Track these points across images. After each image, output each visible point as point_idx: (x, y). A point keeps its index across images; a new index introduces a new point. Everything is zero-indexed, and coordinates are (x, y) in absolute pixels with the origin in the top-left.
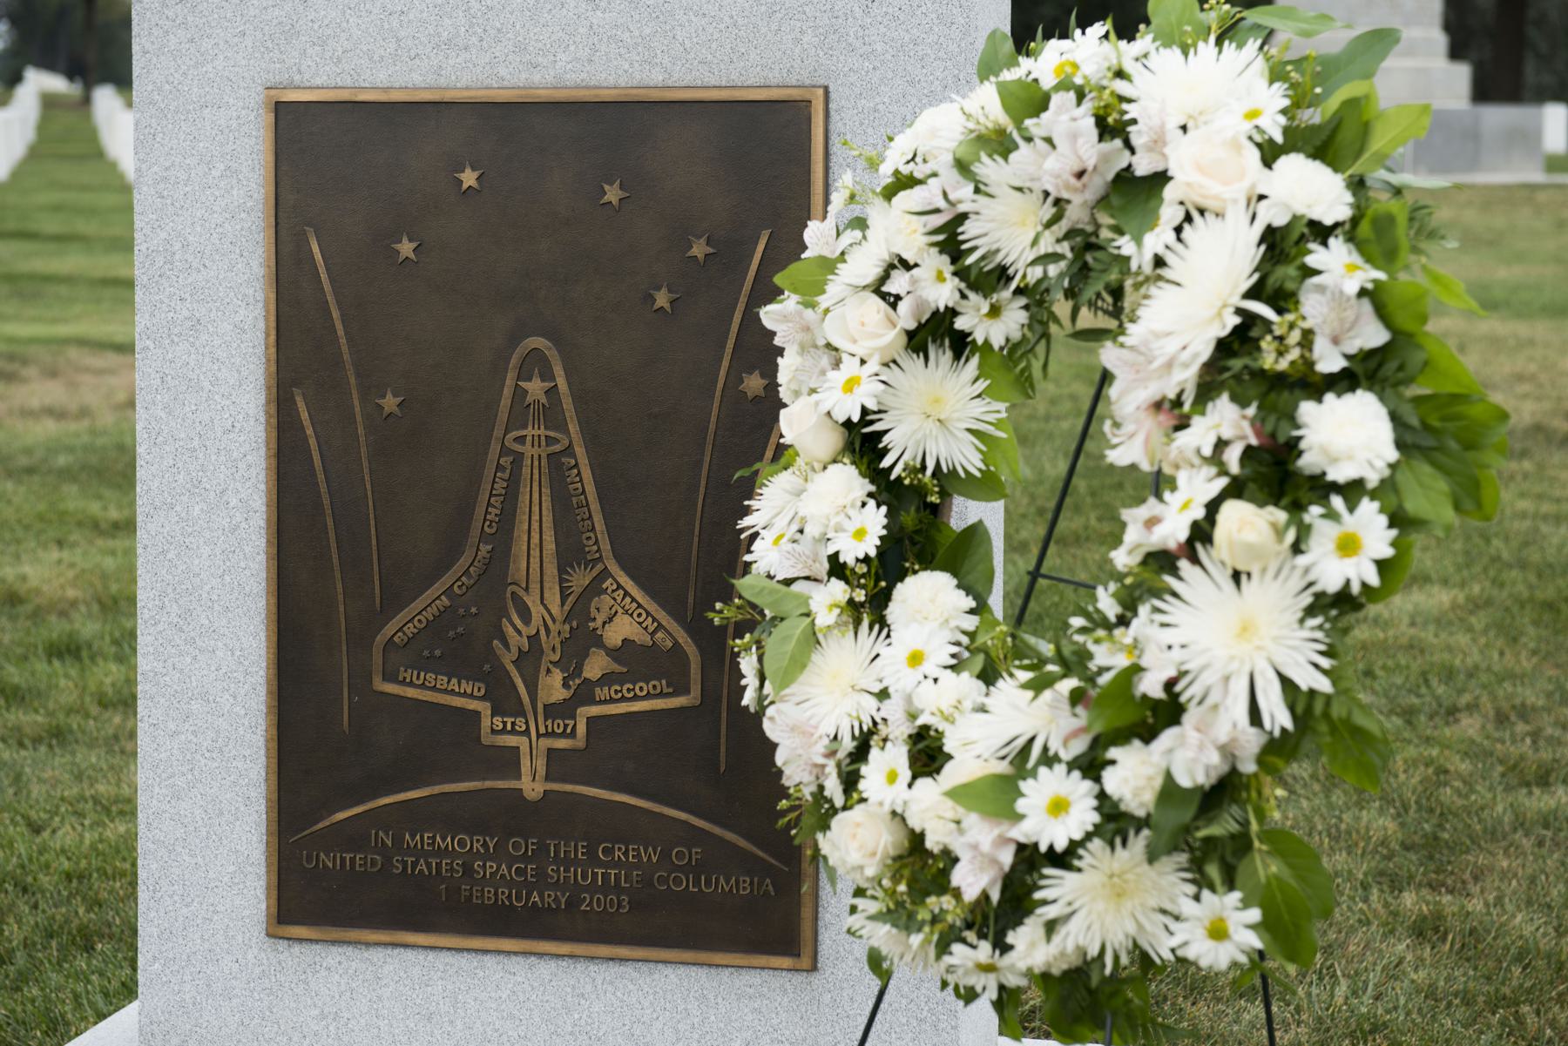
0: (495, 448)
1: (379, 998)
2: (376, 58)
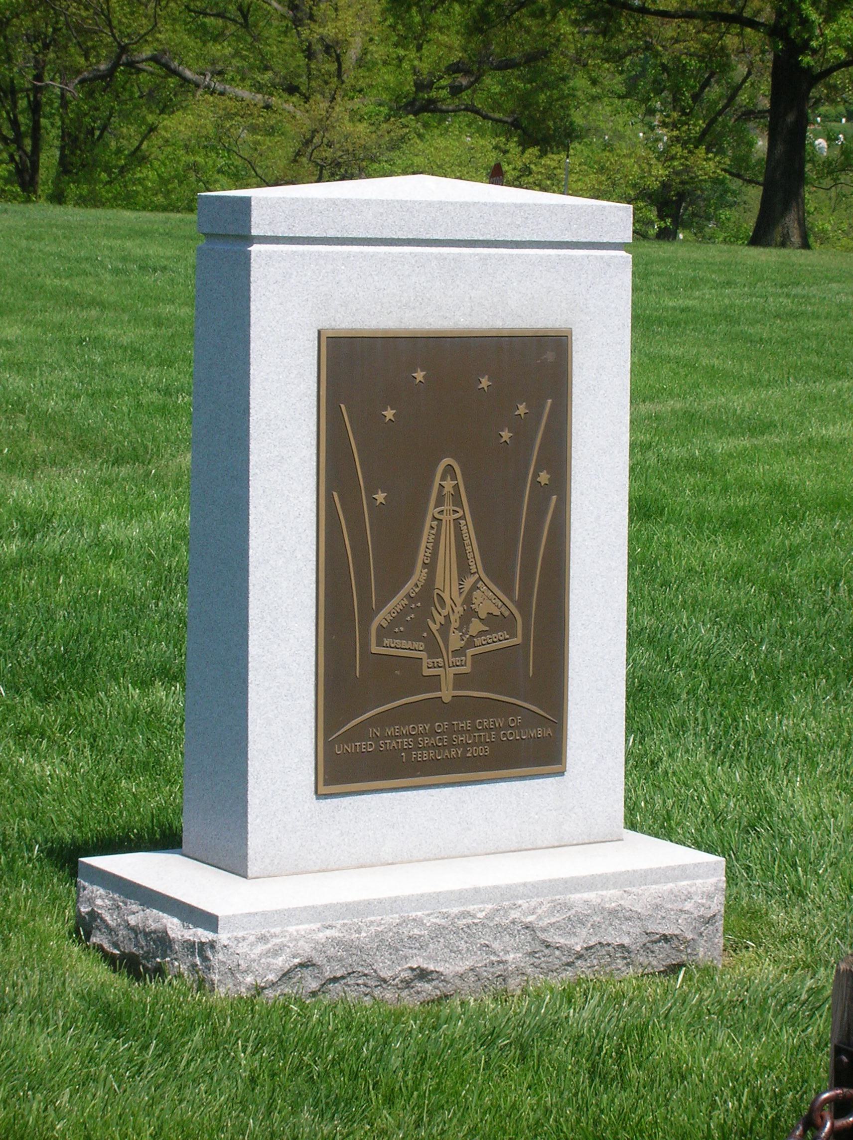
0: (429, 518)
1: (370, 820)
2: (372, 313)
